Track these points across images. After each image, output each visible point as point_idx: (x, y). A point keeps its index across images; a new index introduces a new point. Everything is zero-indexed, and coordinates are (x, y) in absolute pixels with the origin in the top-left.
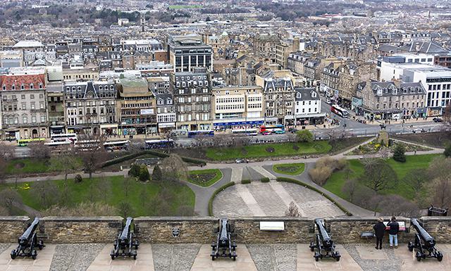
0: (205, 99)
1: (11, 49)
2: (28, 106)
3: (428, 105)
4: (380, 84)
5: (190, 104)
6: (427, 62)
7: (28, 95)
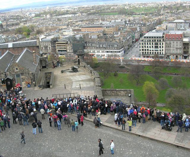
1: (172, 23)
2: (175, 46)
7: (175, 42)
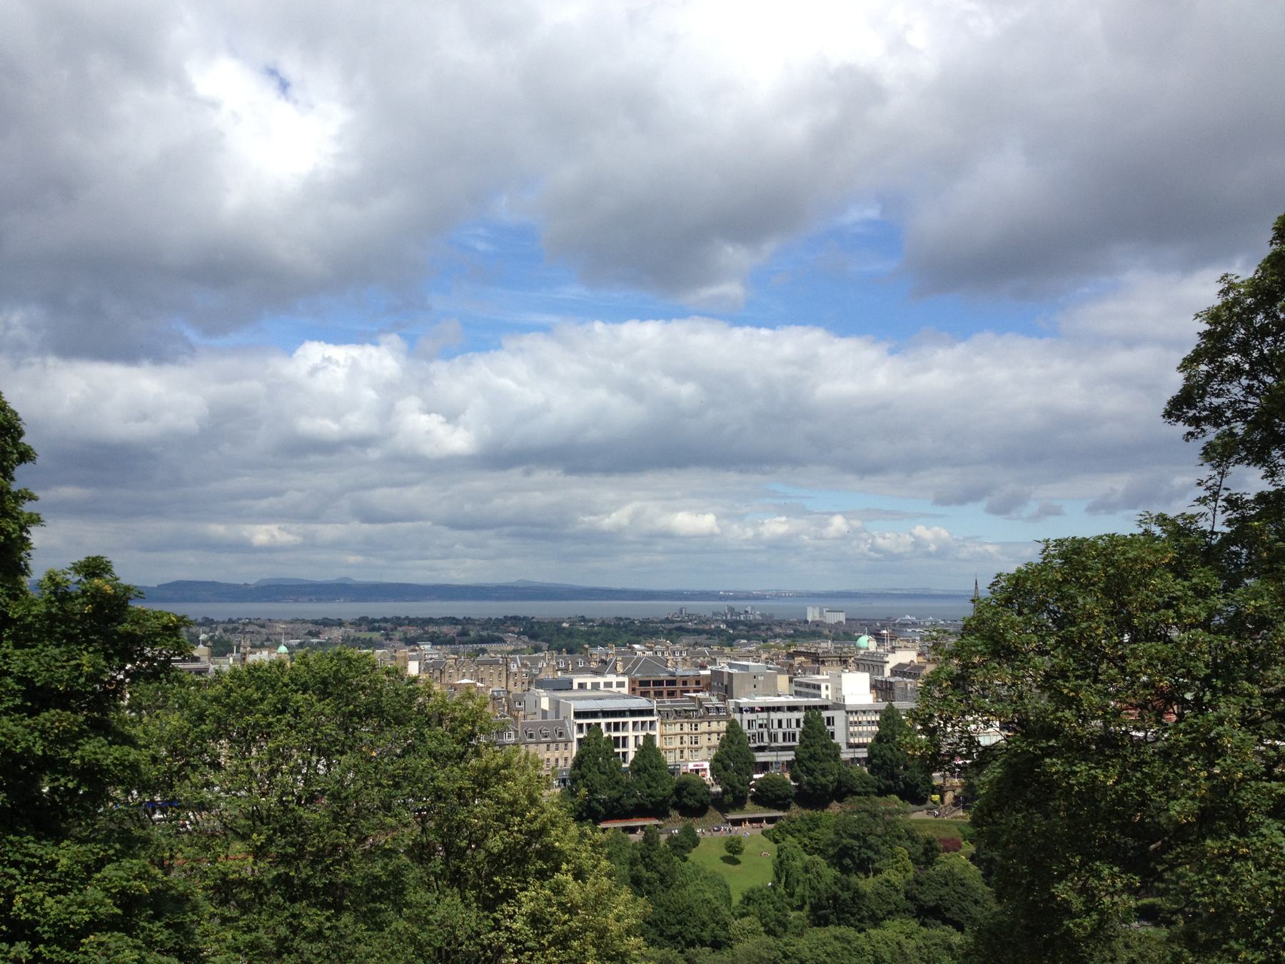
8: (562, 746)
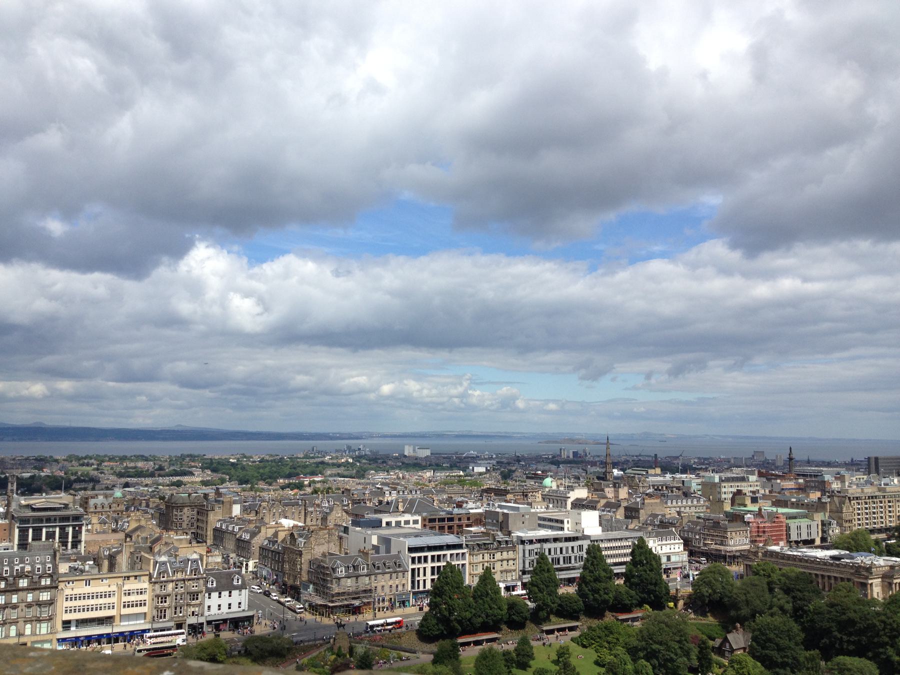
0: (45, 596)
3: (413, 587)
4: (340, 559)
5: (15, 607)
6: (411, 525)
8: (400, 574)
